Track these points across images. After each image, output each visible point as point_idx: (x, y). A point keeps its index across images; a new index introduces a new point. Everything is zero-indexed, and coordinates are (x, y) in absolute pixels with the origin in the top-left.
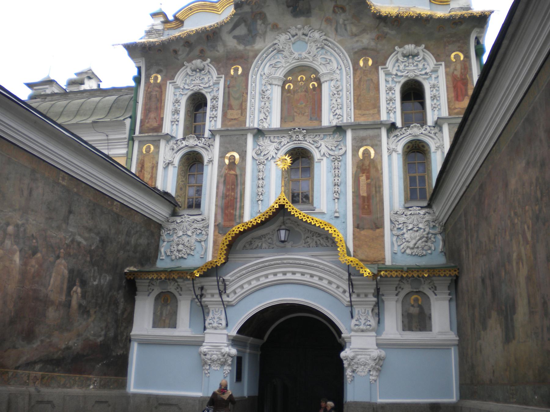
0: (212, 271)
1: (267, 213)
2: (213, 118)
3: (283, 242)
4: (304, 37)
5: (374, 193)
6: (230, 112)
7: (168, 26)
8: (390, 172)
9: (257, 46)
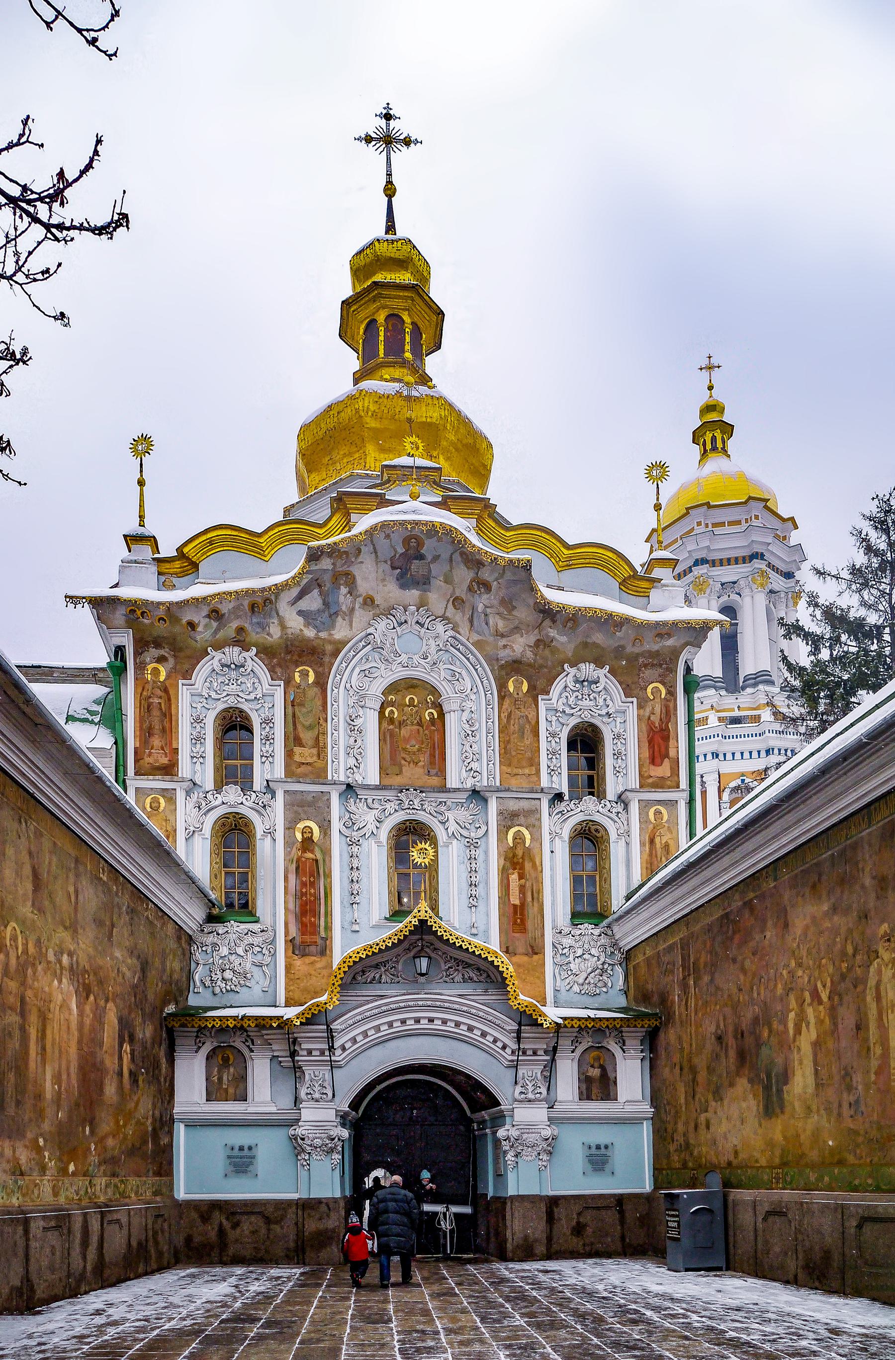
5: (529, 899)
6: (297, 750)
8: (552, 869)
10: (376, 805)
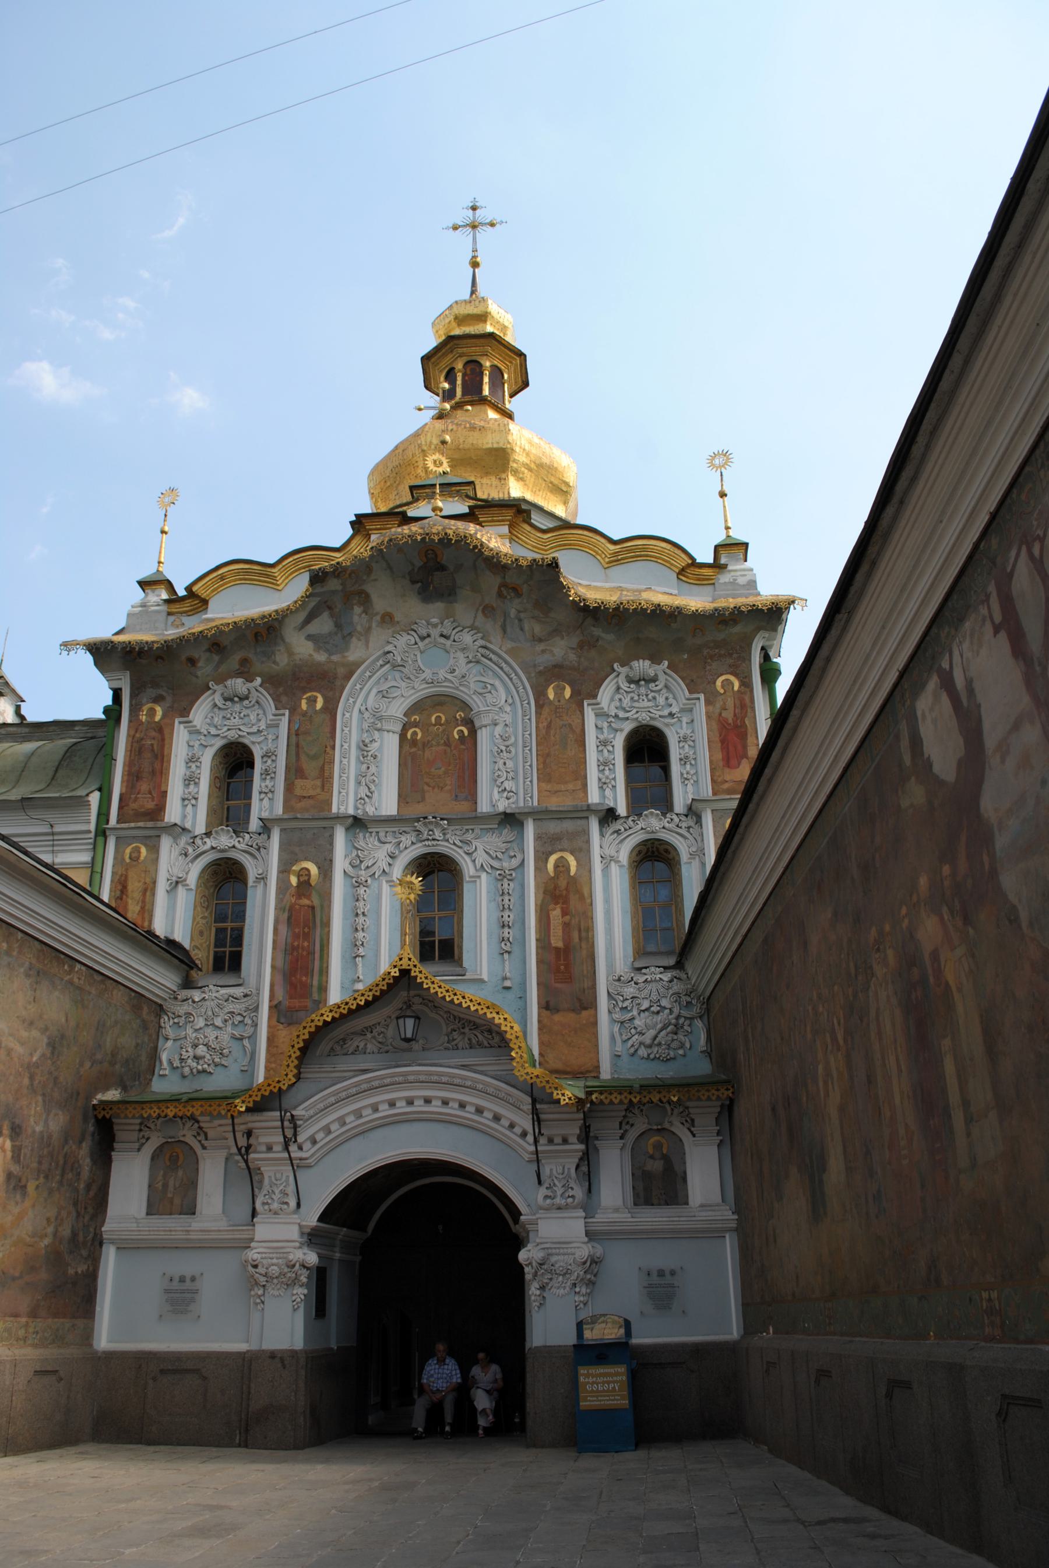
0: (268, 1101)
1: (377, 985)
2: (266, 793)
3: (407, 1040)
4: (442, 640)
5: (576, 940)
6: (299, 783)
7: (175, 608)
8: (608, 900)
9: (352, 656)
10: (389, 839)
